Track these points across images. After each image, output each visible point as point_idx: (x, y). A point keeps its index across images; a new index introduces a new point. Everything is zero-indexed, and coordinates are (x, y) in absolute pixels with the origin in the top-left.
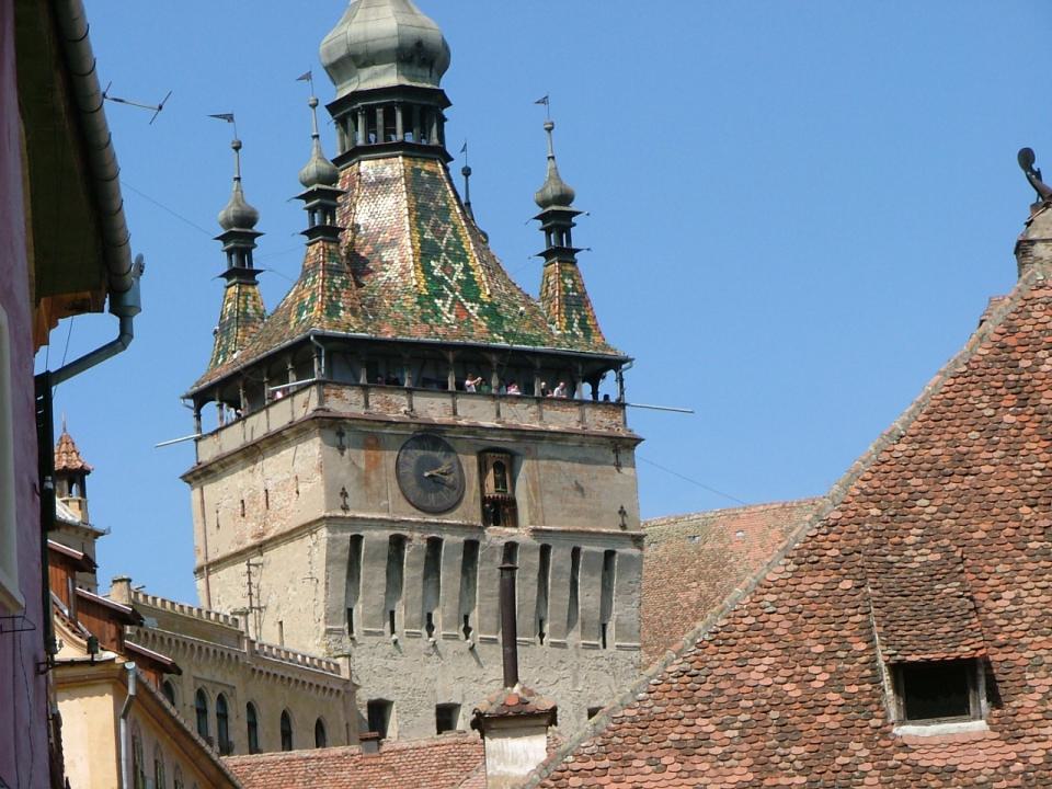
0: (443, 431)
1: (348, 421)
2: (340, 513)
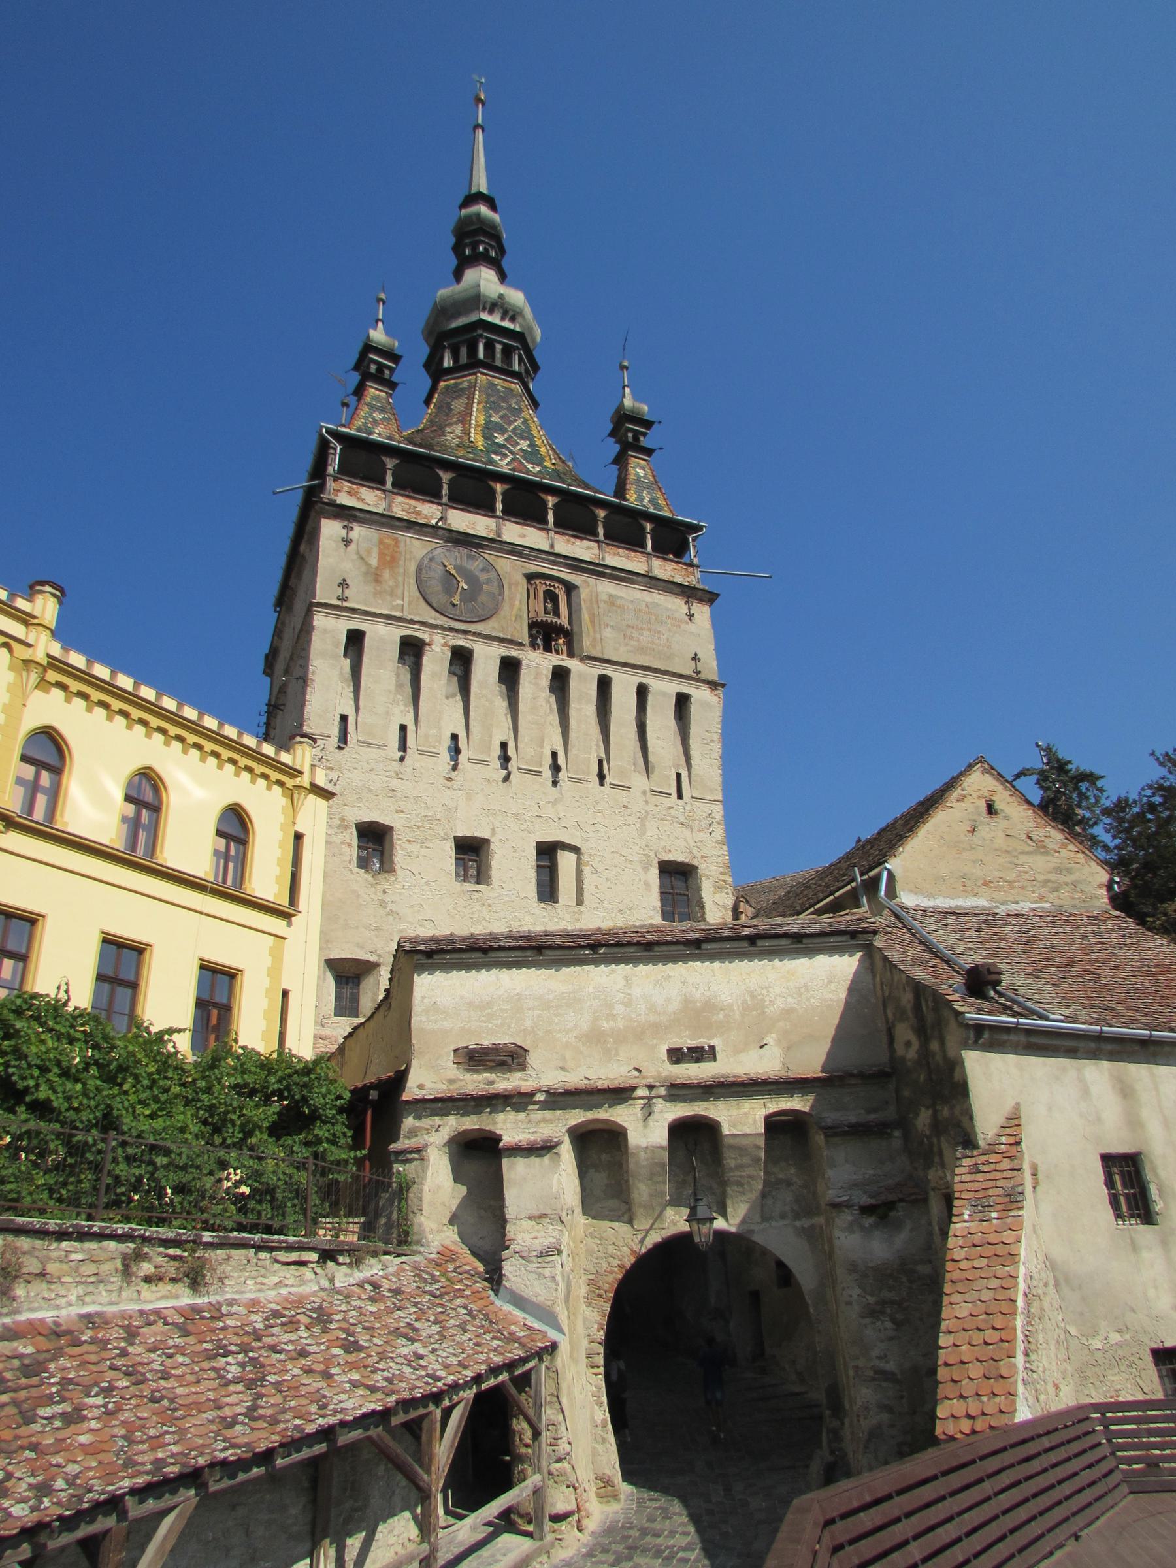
1: (358, 514)
2: (339, 603)
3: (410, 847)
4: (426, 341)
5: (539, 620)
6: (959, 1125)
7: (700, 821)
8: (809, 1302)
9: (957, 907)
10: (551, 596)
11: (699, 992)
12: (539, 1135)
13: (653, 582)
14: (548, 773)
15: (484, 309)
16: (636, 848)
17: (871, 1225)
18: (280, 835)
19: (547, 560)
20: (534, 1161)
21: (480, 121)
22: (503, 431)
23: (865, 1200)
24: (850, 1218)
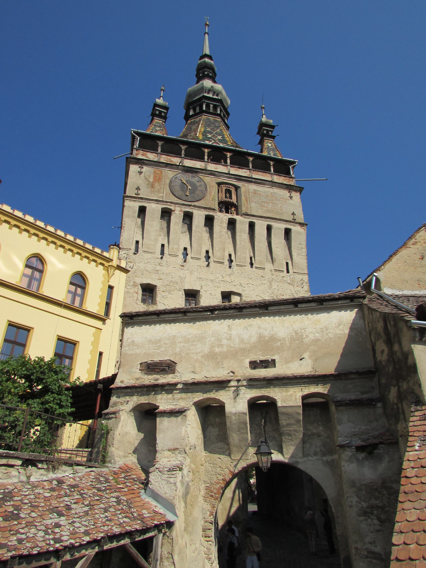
0: (197, 172)
1: (145, 162)
2: (136, 196)
3: (163, 294)
4: (185, 109)
5: (223, 200)
6: (413, 392)
7: (297, 282)
8: (332, 505)
9: (415, 294)
10: (228, 192)
11: (267, 332)
12: (178, 406)
13: (274, 184)
14: (227, 263)
15: (205, 92)
16: (268, 294)
17: (363, 458)
18: (101, 286)
19: (226, 176)
20: (173, 419)
21: (207, 31)
22: (211, 133)
23: (359, 443)
24: (350, 454)
